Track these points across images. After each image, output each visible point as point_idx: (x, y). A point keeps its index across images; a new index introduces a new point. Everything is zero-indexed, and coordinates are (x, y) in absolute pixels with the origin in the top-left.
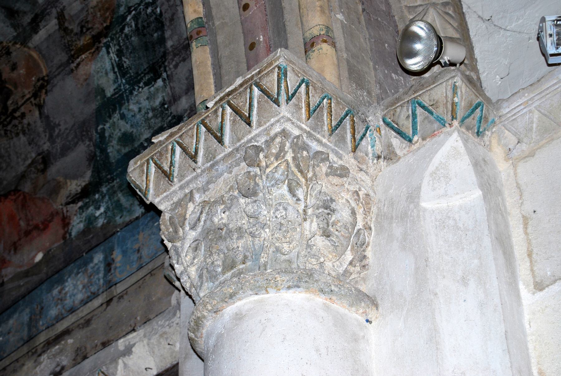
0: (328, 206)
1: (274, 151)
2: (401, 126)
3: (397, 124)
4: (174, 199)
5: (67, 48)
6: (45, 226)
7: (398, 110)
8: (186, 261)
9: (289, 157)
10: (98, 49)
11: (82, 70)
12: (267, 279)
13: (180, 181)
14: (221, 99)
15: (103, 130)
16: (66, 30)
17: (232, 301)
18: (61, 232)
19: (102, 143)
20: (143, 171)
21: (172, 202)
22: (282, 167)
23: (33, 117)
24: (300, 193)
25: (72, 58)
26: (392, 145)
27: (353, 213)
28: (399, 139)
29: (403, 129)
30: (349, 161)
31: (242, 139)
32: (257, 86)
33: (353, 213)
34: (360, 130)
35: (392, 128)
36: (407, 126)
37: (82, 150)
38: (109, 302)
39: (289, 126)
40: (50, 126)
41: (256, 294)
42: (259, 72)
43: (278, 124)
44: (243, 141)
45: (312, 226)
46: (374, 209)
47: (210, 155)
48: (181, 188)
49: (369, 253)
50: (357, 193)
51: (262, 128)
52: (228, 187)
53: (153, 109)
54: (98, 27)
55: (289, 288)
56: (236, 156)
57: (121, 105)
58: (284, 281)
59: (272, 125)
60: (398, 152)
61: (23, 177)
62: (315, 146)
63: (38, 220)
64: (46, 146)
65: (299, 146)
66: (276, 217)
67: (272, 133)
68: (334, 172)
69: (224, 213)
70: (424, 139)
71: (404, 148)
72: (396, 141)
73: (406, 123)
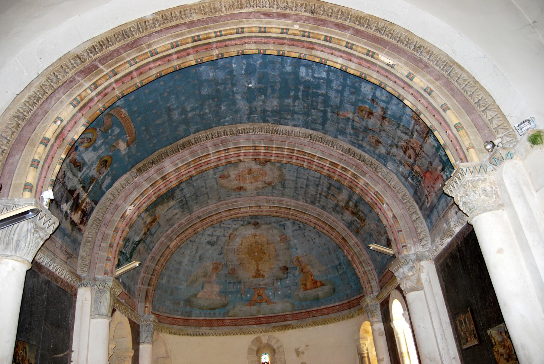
0: (484, 190)
5: (422, 137)
6: (438, 178)
9: (471, 186)
11: (428, 142)
19: (440, 157)
23: (423, 154)
24: (477, 192)
25: (424, 139)
27: (492, 187)
30: (486, 176)
33: (492, 187)
34: (485, 168)
37: (437, 160)
39: (468, 179)
40: (428, 156)
45: (483, 197)
46: (496, 182)
47: (457, 186)
49: (499, 193)
50: (490, 182)
61: (428, 167)
62: (476, 178)
63: (436, 177)
65: (472, 182)
68: (483, 181)
72: (494, 166)
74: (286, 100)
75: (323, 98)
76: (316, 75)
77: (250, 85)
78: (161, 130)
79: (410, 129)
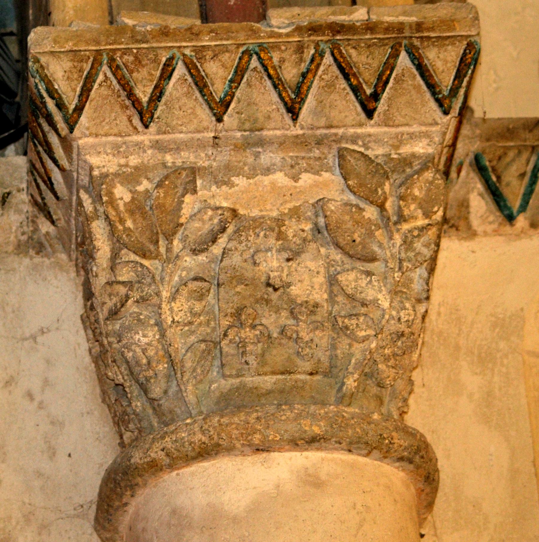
1: (416, 192)
2: (504, 183)
3: (499, 178)
4: (131, 158)
7: (511, 154)
8: (171, 309)
12: (381, 435)
13: (159, 132)
14: (314, 29)
17: (307, 447)
20: (81, 71)
21: (123, 161)
22: (430, 233)
26: (468, 207)
28: (487, 203)
29: (506, 192)
31: (337, 127)
32: (409, 53)
35: (487, 182)
41: (350, 451)
42: (419, 26)
43: (425, 141)
44: (333, 131)
48: (157, 146)
51: (386, 129)
52: (290, 205)
55: (401, 459)
56: (310, 150)
58: (401, 446)
59: (412, 136)
60: (475, 222)
66: (399, 319)
67: (406, 150)
69: (288, 260)
70: (533, 225)
71: (490, 223)
72: (479, 204)
73: (515, 182)
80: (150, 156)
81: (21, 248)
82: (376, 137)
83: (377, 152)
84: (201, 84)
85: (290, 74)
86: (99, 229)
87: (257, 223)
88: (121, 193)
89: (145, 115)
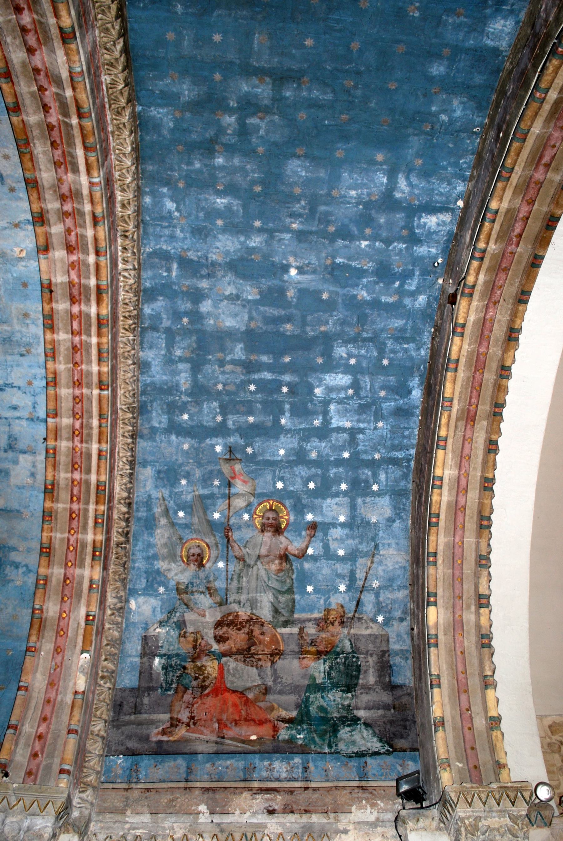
10: (319, 659)
11: (305, 661)
14: (501, 787)
15: (309, 697)
16: (302, 637)
18: (272, 733)
36: (533, 819)
38: (306, 788)
53: (343, 705)
54: (321, 648)
57: (323, 691)
64: (270, 683)
74: (241, 345)
75: (269, 424)
76: (332, 407)
77: (293, 272)
78: (217, 38)
79: (296, 616)
80: (471, 813)
81: (436, 829)
82: (514, 810)
83: (515, 813)
84: (481, 799)
85: (497, 797)
86: (463, 829)
87: (494, 829)
88: (467, 822)
89: (470, 805)
